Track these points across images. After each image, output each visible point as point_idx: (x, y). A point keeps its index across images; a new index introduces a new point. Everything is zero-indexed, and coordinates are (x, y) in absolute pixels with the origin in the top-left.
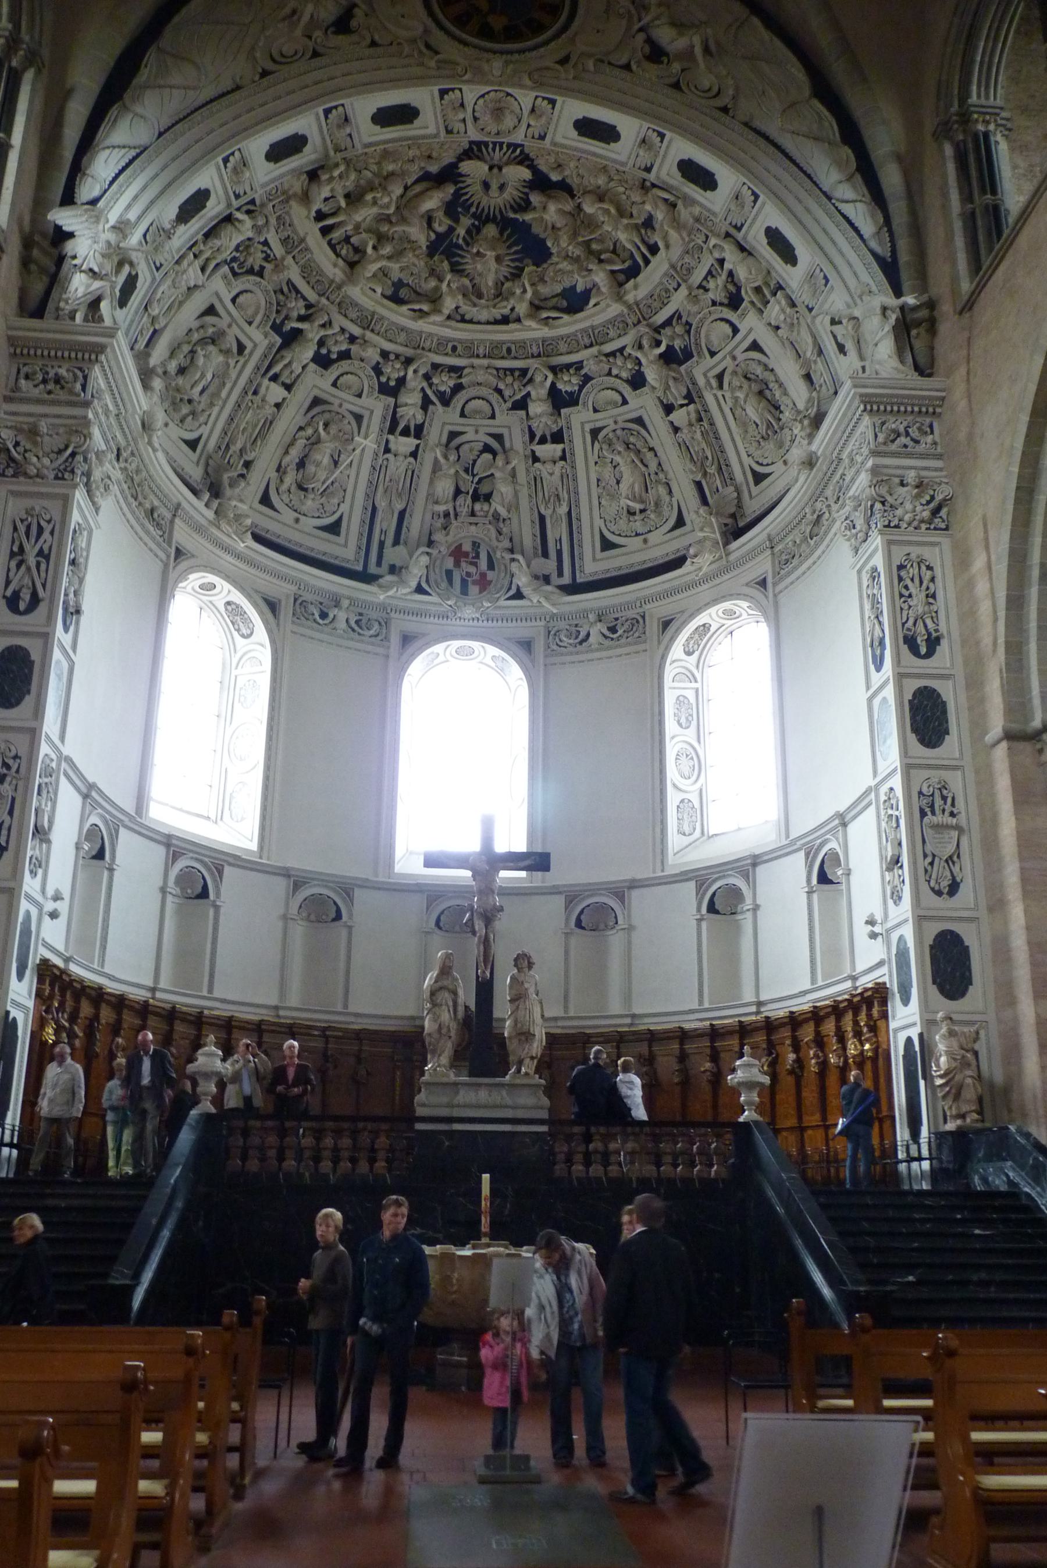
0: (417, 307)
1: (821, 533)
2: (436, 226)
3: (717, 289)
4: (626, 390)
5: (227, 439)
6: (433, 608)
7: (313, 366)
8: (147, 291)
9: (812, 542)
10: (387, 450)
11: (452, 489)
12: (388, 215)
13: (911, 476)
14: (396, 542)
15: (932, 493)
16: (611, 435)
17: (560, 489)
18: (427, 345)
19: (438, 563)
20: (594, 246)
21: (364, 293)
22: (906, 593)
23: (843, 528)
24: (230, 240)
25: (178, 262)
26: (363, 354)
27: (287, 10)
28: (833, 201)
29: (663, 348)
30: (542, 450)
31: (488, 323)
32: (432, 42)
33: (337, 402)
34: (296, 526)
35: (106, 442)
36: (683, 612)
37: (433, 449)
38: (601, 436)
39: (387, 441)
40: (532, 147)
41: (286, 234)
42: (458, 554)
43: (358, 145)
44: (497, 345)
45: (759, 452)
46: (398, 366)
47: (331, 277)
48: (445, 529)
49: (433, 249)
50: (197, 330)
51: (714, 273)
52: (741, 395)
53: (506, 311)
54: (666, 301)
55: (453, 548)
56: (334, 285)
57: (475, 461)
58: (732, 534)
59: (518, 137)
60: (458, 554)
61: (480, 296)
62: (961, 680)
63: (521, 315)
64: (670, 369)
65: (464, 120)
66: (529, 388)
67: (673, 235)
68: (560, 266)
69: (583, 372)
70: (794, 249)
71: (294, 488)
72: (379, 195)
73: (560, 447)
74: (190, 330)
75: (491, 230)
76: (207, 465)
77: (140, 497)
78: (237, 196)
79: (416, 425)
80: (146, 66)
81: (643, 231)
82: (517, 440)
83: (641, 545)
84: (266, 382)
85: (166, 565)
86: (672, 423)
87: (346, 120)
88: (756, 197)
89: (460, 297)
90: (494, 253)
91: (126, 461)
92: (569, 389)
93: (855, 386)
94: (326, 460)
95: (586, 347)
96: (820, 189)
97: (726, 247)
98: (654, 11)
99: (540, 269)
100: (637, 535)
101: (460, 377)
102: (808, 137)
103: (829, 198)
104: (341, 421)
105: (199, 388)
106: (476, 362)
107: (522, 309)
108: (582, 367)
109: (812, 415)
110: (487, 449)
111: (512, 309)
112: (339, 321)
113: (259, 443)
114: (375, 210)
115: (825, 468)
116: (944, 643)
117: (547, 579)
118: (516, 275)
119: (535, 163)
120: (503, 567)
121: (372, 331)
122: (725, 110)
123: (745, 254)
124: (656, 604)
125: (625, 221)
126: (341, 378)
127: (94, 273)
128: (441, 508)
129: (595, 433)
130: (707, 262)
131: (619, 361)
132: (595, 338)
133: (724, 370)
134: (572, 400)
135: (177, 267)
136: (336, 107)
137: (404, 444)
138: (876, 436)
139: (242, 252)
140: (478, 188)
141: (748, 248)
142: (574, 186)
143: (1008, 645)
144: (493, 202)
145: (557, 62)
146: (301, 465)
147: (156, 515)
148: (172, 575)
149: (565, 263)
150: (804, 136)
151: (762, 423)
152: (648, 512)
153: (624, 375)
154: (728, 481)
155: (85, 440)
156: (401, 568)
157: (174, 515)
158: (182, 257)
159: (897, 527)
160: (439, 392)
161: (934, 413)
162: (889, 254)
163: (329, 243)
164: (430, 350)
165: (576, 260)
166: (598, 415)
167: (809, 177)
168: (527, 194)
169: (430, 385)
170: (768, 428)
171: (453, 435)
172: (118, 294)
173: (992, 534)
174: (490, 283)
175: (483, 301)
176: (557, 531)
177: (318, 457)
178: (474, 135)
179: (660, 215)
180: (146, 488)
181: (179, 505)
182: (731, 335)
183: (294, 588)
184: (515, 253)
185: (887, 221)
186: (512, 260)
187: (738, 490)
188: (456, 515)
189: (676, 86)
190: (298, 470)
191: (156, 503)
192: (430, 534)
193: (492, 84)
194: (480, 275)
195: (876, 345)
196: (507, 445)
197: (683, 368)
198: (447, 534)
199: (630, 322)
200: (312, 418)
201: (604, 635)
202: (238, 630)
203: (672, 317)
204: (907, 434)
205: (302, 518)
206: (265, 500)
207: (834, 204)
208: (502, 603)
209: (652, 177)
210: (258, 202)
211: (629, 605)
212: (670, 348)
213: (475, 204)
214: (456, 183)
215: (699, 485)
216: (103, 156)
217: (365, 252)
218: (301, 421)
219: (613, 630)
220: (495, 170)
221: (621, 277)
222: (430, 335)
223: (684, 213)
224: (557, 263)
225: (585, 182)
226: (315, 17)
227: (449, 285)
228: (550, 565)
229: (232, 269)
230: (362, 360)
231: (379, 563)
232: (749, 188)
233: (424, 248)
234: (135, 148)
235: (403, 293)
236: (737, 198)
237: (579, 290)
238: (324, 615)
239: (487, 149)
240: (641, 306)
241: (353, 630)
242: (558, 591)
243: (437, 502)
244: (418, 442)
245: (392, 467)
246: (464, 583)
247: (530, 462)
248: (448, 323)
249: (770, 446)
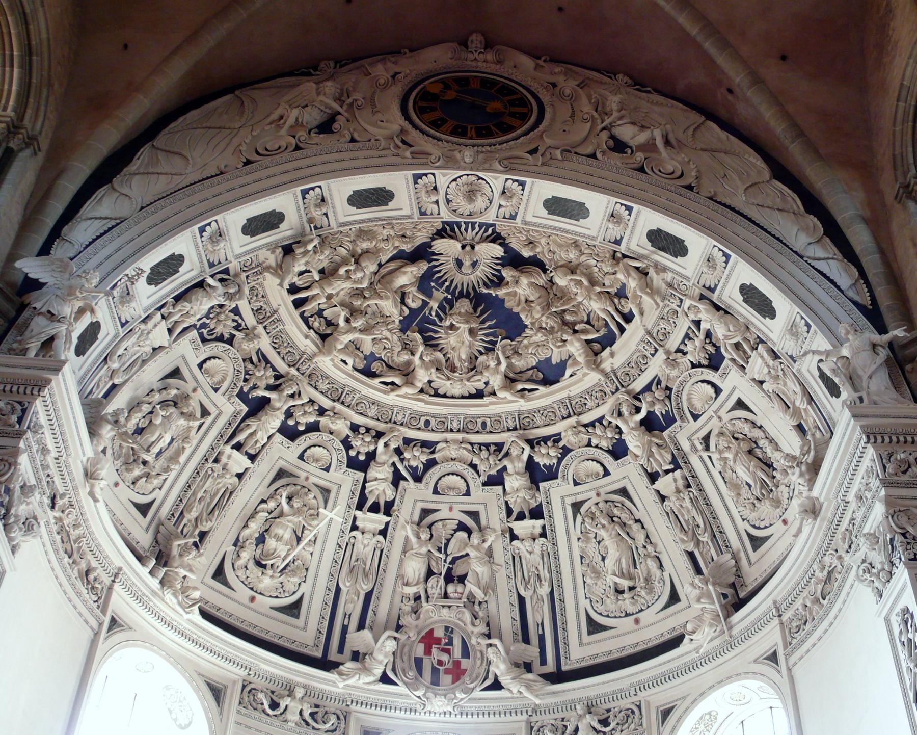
0: (389, 380)
1: (835, 588)
2: (409, 301)
3: (695, 351)
4: (608, 460)
5: (182, 506)
6: (399, 701)
7: (279, 438)
8: (109, 345)
9: (825, 602)
10: (354, 528)
11: (423, 571)
12: (362, 290)
14: (361, 626)
16: (593, 509)
17: (541, 568)
18: (400, 418)
19: (406, 649)
20: (568, 317)
21: (335, 366)
23: (861, 572)
24: (201, 305)
25: (144, 321)
26: (333, 427)
27: (275, 116)
28: (805, 259)
29: (643, 414)
30: (521, 527)
31: (463, 397)
32: (408, 139)
33: (303, 475)
34: (252, 605)
35: (38, 479)
36: (684, 698)
37: (404, 527)
38: (583, 509)
39: (355, 518)
40: (503, 228)
41: (258, 304)
42: (429, 640)
43: (333, 223)
44: (473, 420)
45: (754, 514)
46: (368, 439)
47: (303, 348)
48: (415, 613)
49: (405, 325)
50: (160, 391)
51: (691, 335)
52: (729, 455)
53: (480, 385)
54: (643, 368)
55: (423, 634)
56: (305, 356)
57: (448, 540)
58: (732, 605)
59: (489, 218)
60: (429, 640)
61: (453, 369)
63: (496, 388)
64: (654, 436)
65: (437, 202)
66: (506, 462)
67: (647, 300)
68: (535, 339)
69: (561, 444)
71: (251, 565)
72: (352, 268)
73: (540, 522)
74: (152, 391)
75: (464, 305)
76: (157, 532)
77: (76, 556)
78: (211, 265)
79: (386, 502)
80: (138, 159)
81: (616, 301)
82: (494, 517)
83: (633, 626)
84: (228, 449)
85: (97, 634)
86: (658, 492)
87: (323, 200)
88: (728, 257)
89: (433, 370)
90: (467, 326)
91: (63, 512)
92: (547, 462)
94: (287, 535)
95: (564, 418)
96: (791, 249)
97: (701, 306)
98: (615, 114)
99: (513, 343)
100: (627, 615)
101: (433, 452)
103: (802, 257)
104: (306, 494)
105: (156, 450)
106: (450, 436)
107: (496, 381)
108: (560, 439)
109: (810, 461)
110: (462, 527)
111: (487, 383)
112: (309, 392)
113: (217, 513)
114: (348, 285)
115: (829, 515)
117: (528, 667)
118: (490, 350)
119: (507, 242)
120: (479, 655)
121: (343, 403)
122: (690, 188)
123: (722, 312)
124: (653, 690)
125: (598, 289)
126: (308, 451)
127: (53, 315)
128: (411, 591)
129: (576, 506)
130: (684, 325)
131: (598, 430)
132: (572, 409)
133: (710, 433)
134: (551, 474)
135: (142, 326)
136: (313, 189)
137: (372, 521)
138: (885, 467)
139: (212, 319)
140: (452, 265)
141: (723, 307)
142: (546, 261)
144: (466, 279)
145: (527, 152)
146: (261, 540)
147: (91, 577)
148: (101, 647)
149: (539, 335)
150: (768, 207)
151: (756, 483)
152: (638, 589)
153: (604, 444)
154: (724, 549)
155: (10, 468)
156: (365, 654)
157: (114, 581)
158: (148, 317)
160: (411, 467)
162: (870, 302)
163: (302, 315)
164: (402, 424)
165: (551, 331)
166: (579, 489)
167: (778, 239)
168: (499, 271)
169: (402, 460)
170: (762, 487)
171: (426, 512)
172: (75, 341)
174: (464, 357)
175: (456, 374)
176: (538, 614)
177: (277, 530)
178: (447, 216)
179: (632, 284)
180: (85, 548)
181: (120, 569)
182: (714, 395)
183: (243, 673)
184: (489, 327)
185: (863, 274)
186: (485, 335)
187: (735, 557)
188: (428, 598)
189: (641, 170)
190: (257, 546)
191: (94, 564)
192: (399, 619)
193: (464, 169)
194: (453, 349)
196: (483, 522)
197: (666, 434)
198: (418, 618)
199: (607, 390)
200: (276, 490)
201: (594, 729)
202: (175, 720)
203: (650, 384)
205: (258, 597)
206: (219, 574)
207: (806, 261)
208: (478, 693)
209: (623, 248)
210: (232, 272)
211: (621, 694)
212: (649, 413)
213: (449, 280)
214: (429, 262)
215: (691, 555)
216: (84, 225)
217: (338, 325)
218: (263, 492)
219: (605, 722)
220: (468, 248)
221: (597, 346)
222: (403, 409)
223: (656, 279)
224: (531, 337)
225: (557, 257)
226: (300, 120)
227: (421, 358)
228: (532, 652)
229: (201, 336)
230: (331, 433)
231: (341, 650)
232: (720, 250)
233: (397, 322)
234: (116, 219)
235: (376, 367)
236: (708, 261)
237: (554, 362)
238: (274, 705)
239: (459, 228)
240: (619, 374)
241: (307, 724)
242: (541, 679)
243: (407, 584)
244: (388, 519)
245: (359, 547)
246: (435, 671)
247: (508, 540)
248: (421, 396)
249: (765, 508)
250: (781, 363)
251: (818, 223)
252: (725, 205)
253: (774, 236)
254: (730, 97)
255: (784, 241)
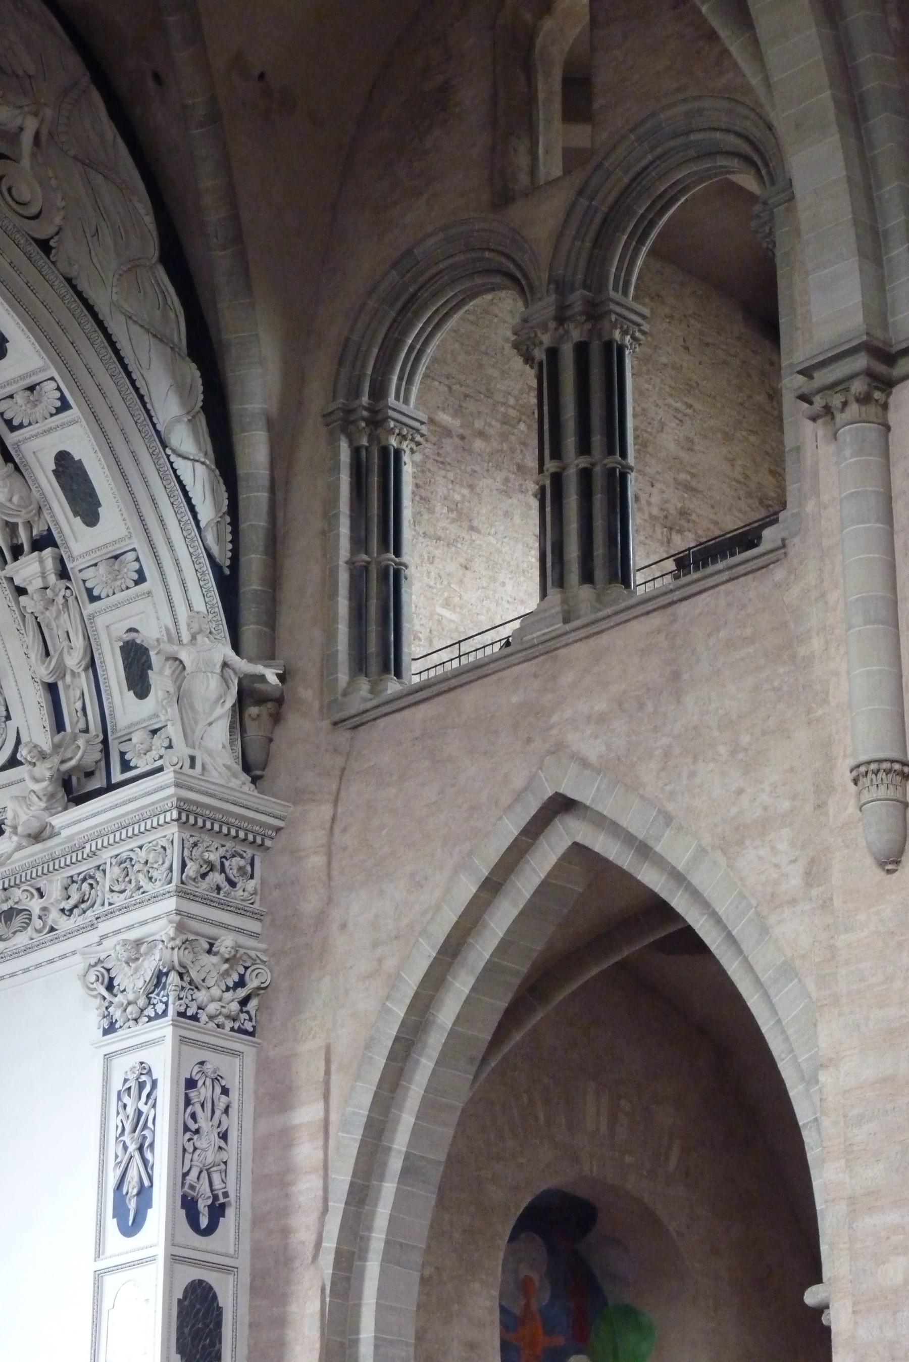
13: (226, 943)
15: (242, 971)
22: (194, 1127)
28: (168, 451)
62: (245, 1278)
70: (99, 505)
93: (177, 785)
96: (154, 425)
102: (148, 331)
103: (164, 446)
115: (58, 851)
116: (230, 1212)
138: (184, 865)
143: (339, 1254)
159: (194, 1018)
161: (262, 845)
162: (228, 563)
167: (141, 397)
173: (335, 1078)
195: (210, 724)
204: (223, 870)
207: (168, 456)
232: (58, 389)
250: (67, 588)
251: (200, 381)
252: (80, 295)
253: (137, 390)
254: (150, 84)
255: (149, 406)
